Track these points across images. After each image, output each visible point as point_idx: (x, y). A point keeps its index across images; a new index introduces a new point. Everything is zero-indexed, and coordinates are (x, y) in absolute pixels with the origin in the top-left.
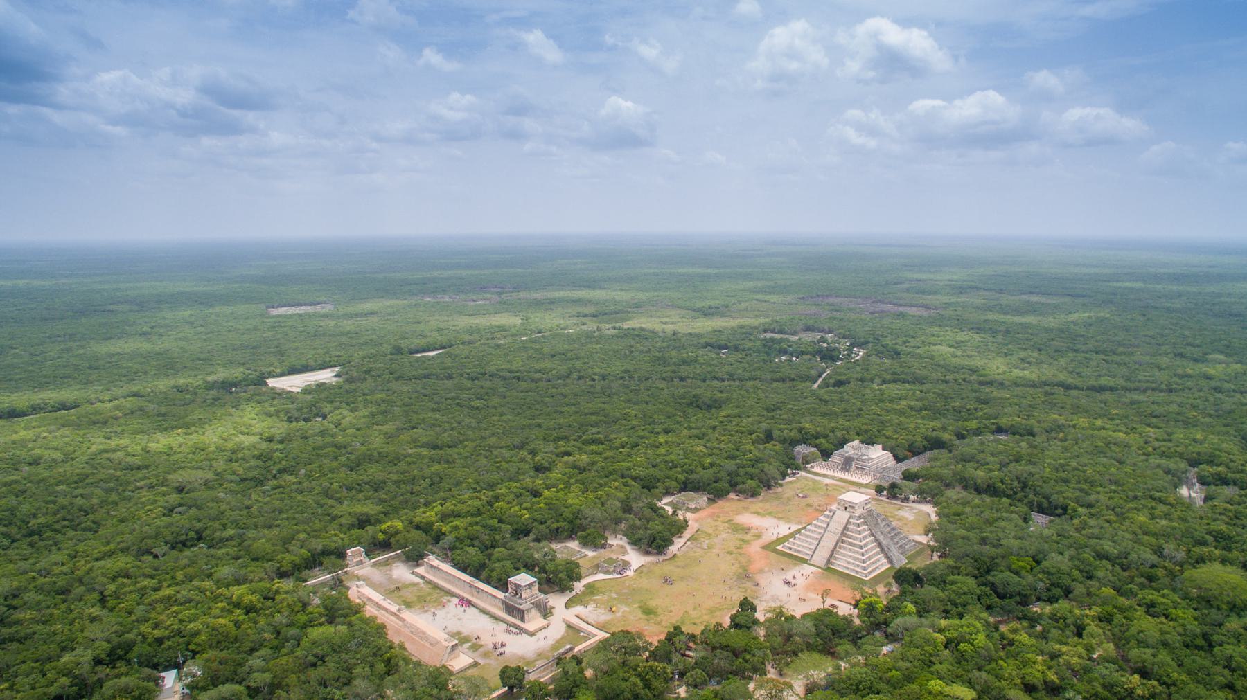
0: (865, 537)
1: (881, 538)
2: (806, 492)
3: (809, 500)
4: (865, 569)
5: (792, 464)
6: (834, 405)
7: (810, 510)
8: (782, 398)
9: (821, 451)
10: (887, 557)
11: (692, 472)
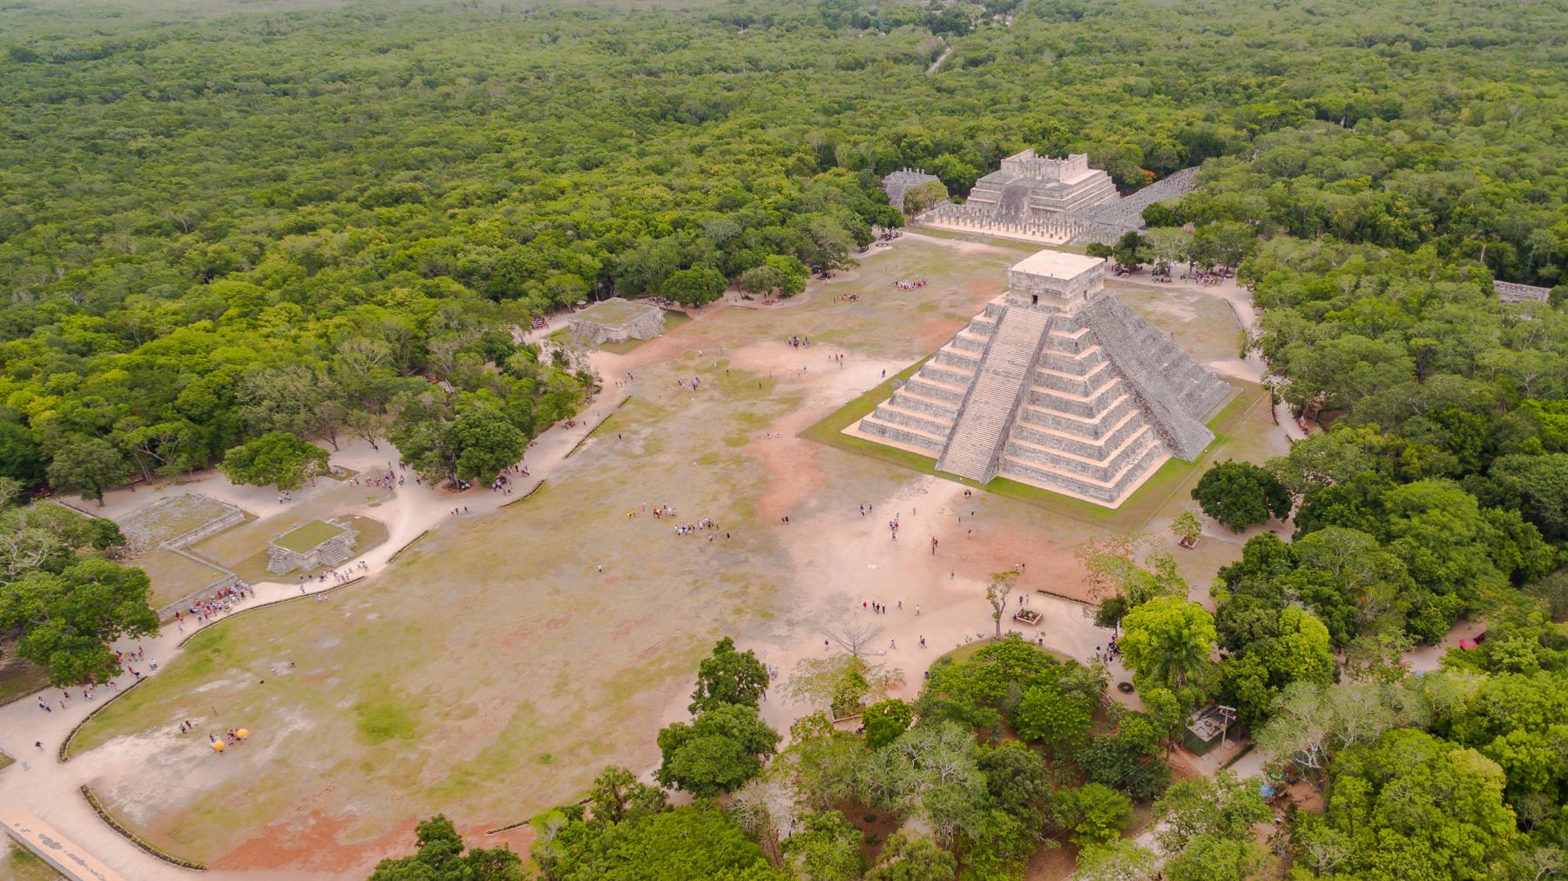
0: (1097, 381)
1: (1141, 378)
2: (919, 277)
3: (927, 294)
4: (1105, 475)
5: (877, 217)
6: (968, 95)
7: (931, 318)
8: (857, 89)
9: (947, 183)
10: (1162, 432)
11: (625, 246)
